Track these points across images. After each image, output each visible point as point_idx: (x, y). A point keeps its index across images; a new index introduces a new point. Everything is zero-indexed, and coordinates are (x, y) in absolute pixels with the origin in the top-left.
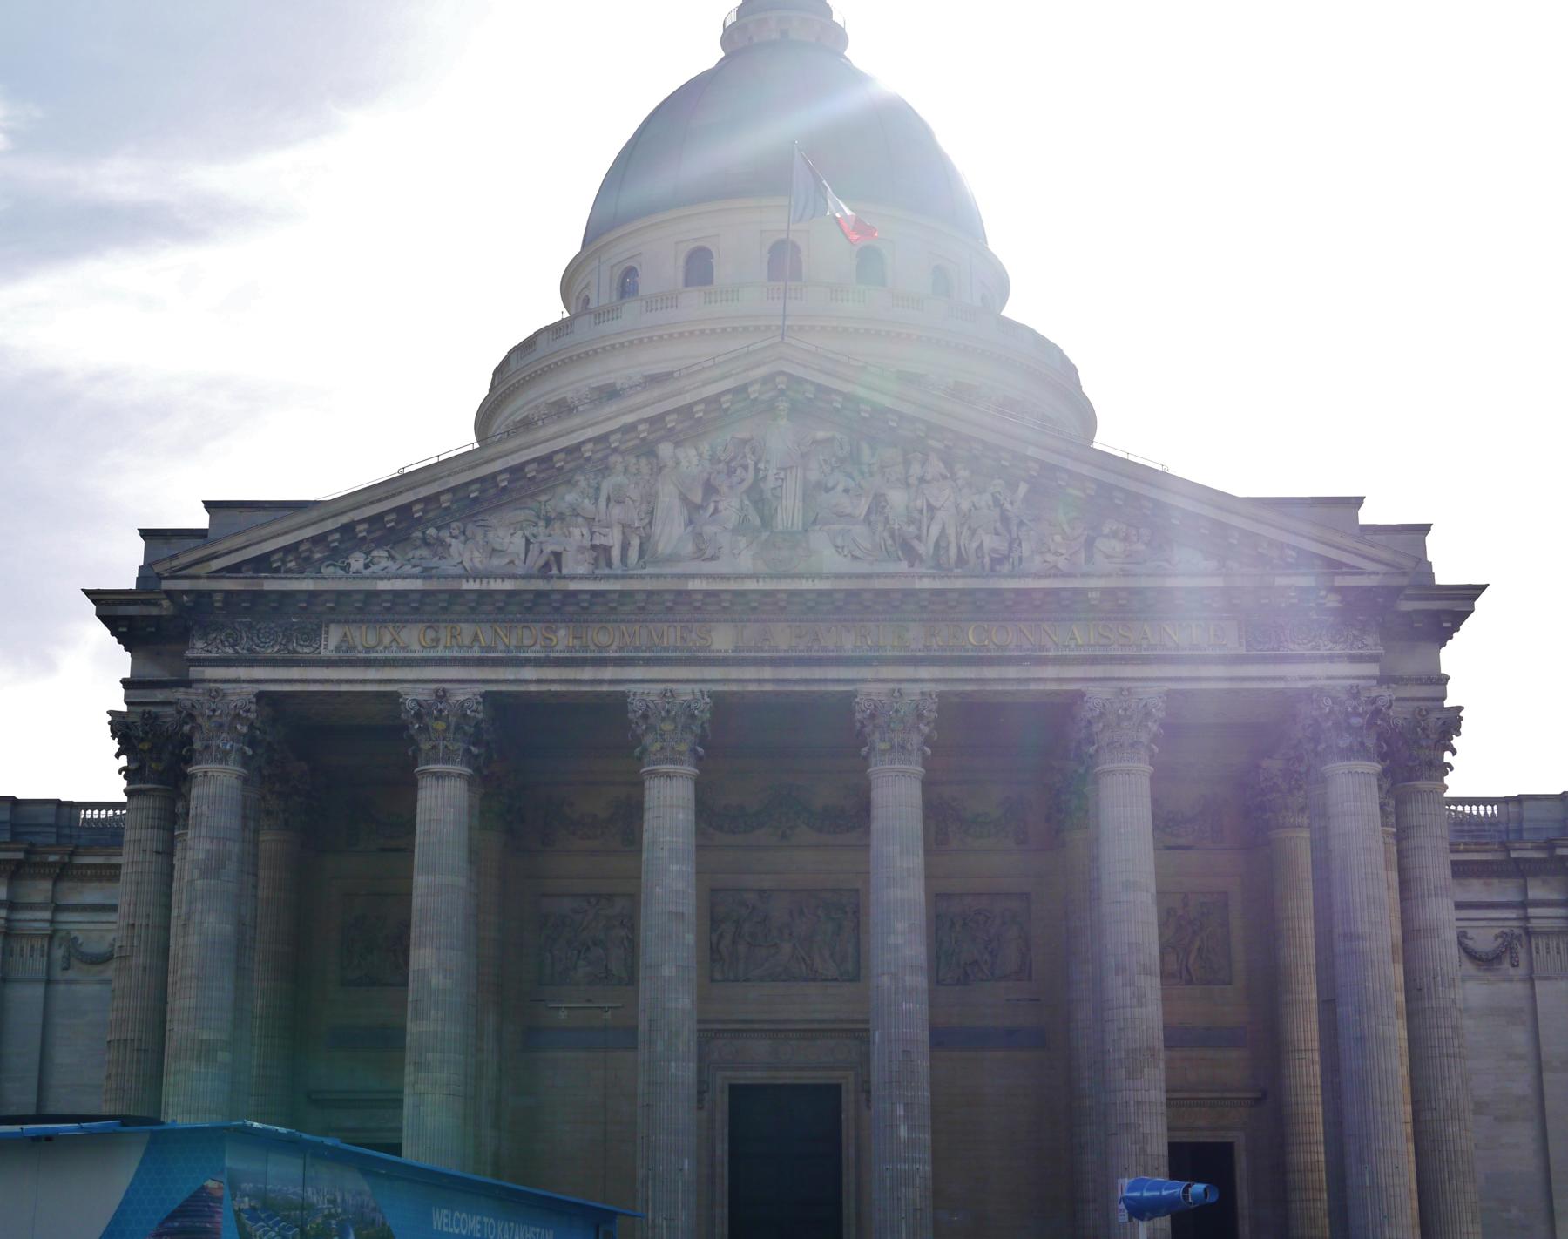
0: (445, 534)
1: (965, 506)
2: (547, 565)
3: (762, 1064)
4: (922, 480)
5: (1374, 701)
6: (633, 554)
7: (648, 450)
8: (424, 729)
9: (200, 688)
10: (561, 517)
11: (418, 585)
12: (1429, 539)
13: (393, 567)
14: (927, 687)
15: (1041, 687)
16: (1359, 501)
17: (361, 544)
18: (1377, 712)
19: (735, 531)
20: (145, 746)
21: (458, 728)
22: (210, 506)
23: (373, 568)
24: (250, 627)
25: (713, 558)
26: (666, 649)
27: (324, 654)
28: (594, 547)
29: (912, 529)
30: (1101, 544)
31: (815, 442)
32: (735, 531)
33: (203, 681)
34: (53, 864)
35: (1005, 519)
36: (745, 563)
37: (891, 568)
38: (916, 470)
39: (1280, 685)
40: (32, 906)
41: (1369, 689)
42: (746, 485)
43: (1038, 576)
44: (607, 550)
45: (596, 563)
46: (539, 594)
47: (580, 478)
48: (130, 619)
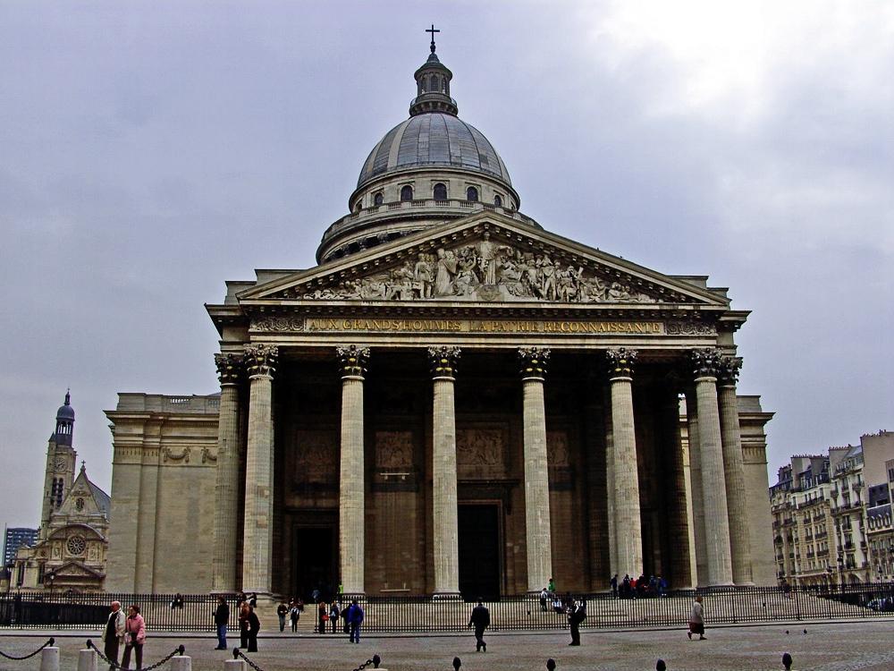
0: (353, 283)
1: (559, 276)
2: (394, 297)
4: (542, 266)
5: (715, 354)
6: (429, 292)
7: (434, 252)
9: (253, 344)
10: (400, 278)
11: (344, 304)
12: (729, 295)
14: (546, 347)
15: (589, 347)
16: (707, 278)
18: (716, 359)
20: (230, 368)
21: (360, 362)
22: (257, 272)
23: (326, 297)
24: (275, 320)
25: (461, 295)
26: (442, 330)
28: (413, 290)
29: (539, 285)
30: (611, 292)
31: (500, 250)
33: (255, 341)
34: (160, 420)
35: (574, 282)
36: (474, 297)
38: (539, 262)
39: (680, 348)
40: (153, 437)
41: (713, 350)
42: (474, 265)
43: (588, 304)
45: (414, 297)
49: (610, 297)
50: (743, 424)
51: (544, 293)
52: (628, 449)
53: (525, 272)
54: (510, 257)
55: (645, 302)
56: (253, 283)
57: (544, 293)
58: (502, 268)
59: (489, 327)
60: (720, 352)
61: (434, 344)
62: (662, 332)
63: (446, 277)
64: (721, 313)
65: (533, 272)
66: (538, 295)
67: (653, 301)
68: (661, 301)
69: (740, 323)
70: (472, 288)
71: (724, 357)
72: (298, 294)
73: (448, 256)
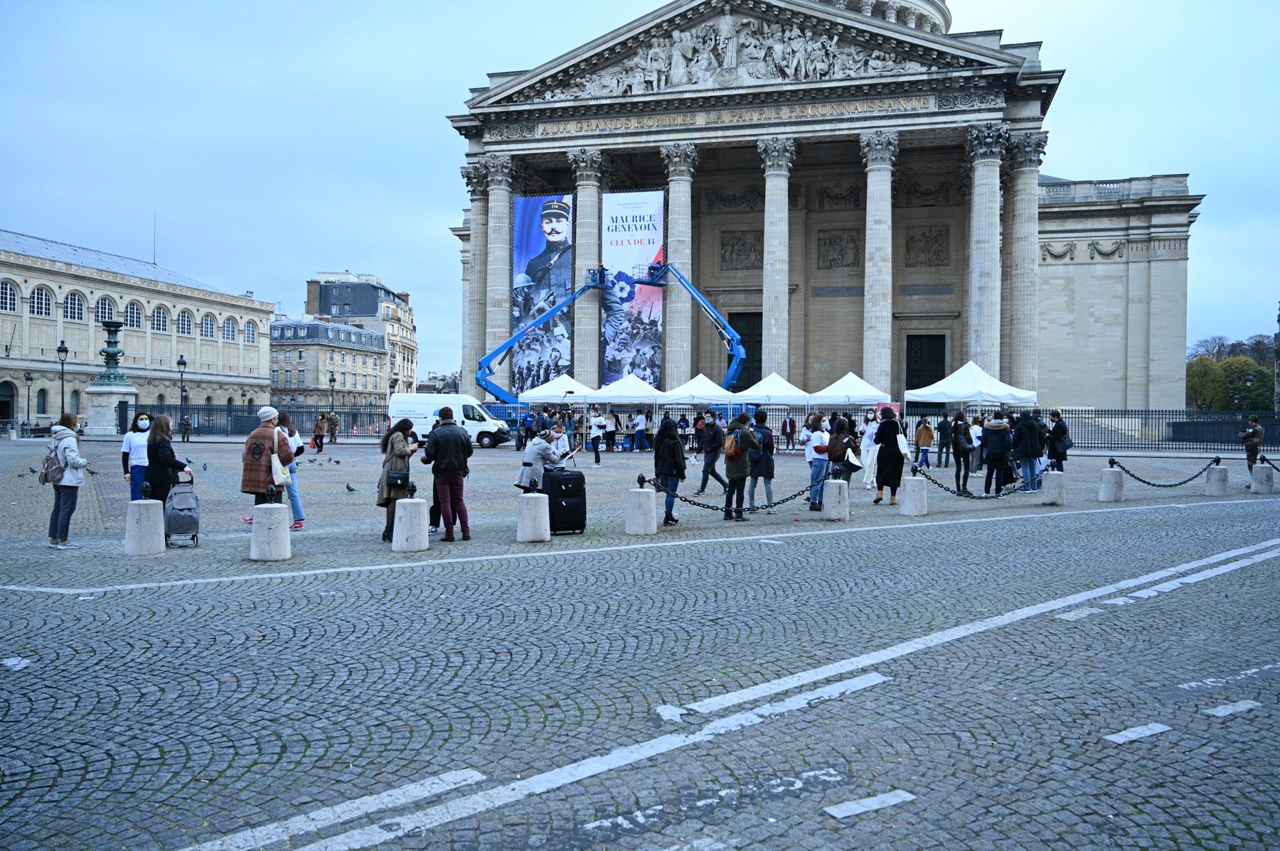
2: (626, 91)
3: (740, 304)
6: (663, 83)
7: (668, 35)
8: (578, 167)
10: (632, 69)
11: (571, 104)
13: (563, 97)
17: (549, 88)
18: (1000, 136)
19: (706, 70)
27: (537, 137)
29: (785, 63)
30: (872, 63)
32: (706, 70)
36: (710, 85)
37: (774, 82)
38: (787, 34)
44: (651, 82)
46: (621, 104)
47: (640, 51)
48: (465, 127)
49: (870, 70)
50: (1043, 216)
51: (790, 71)
52: (879, 249)
53: (770, 48)
54: (754, 33)
55: (914, 71)
56: (486, 89)
57: (790, 71)
58: (743, 46)
59: (727, 117)
60: (1005, 127)
61: (666, 142)
62: (932, 106)
63: (682, 62)
64: (1012, 76)
65: (778, 48)
66: (784, 75)
67: (924, 69)
68: (934, 69)
69: (1052, 89)
70: (708, 74)
71: (1023, 132)
72: (528, 97)
73: (685, 39)
